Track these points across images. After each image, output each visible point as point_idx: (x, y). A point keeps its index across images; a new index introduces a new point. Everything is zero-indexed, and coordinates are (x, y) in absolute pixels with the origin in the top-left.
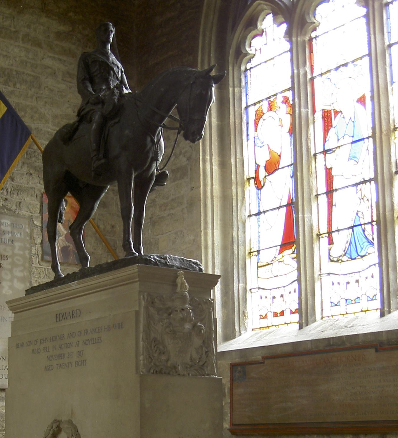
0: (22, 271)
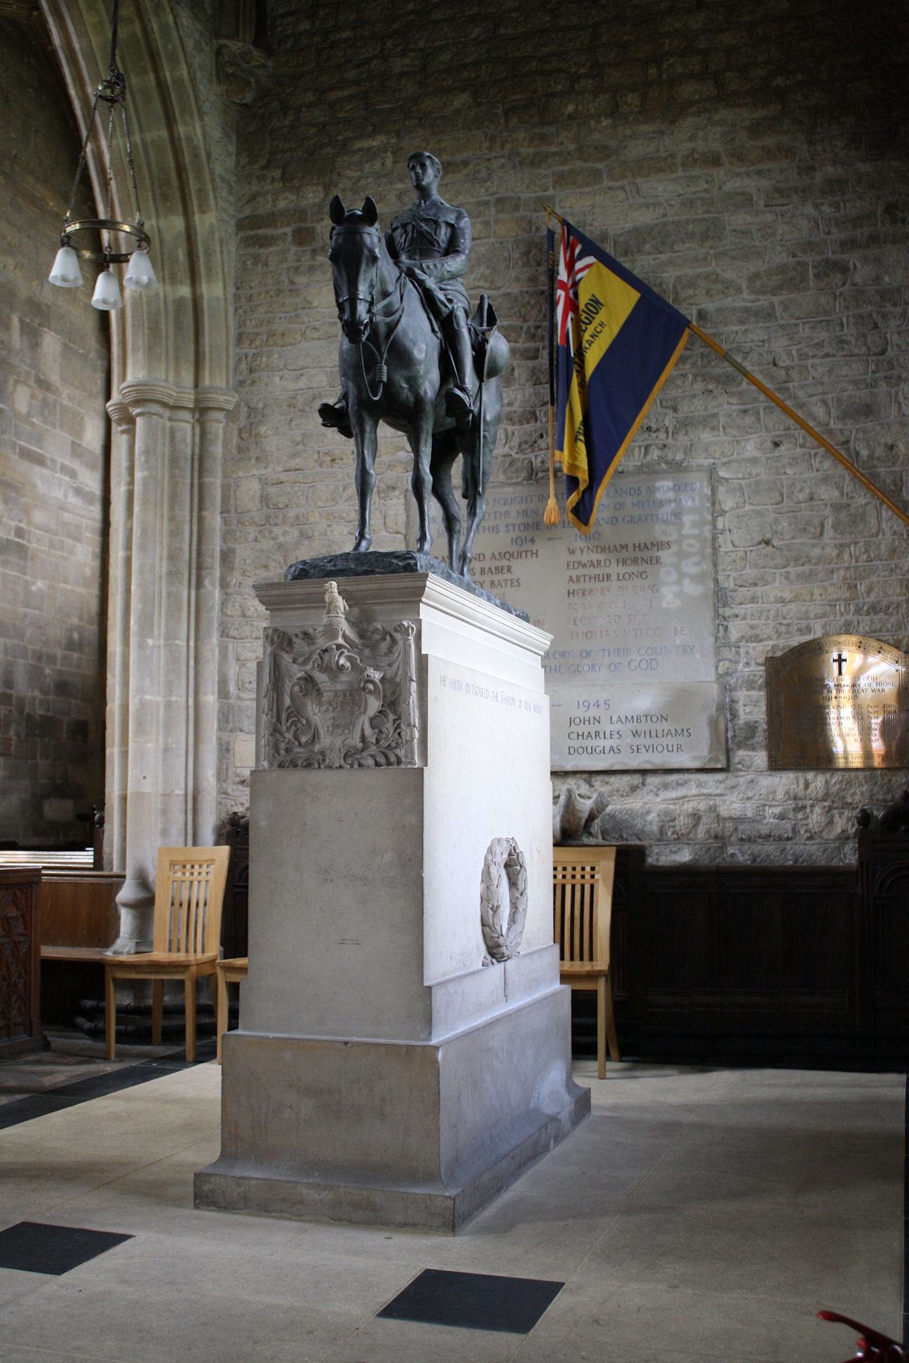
0: (697, 564)
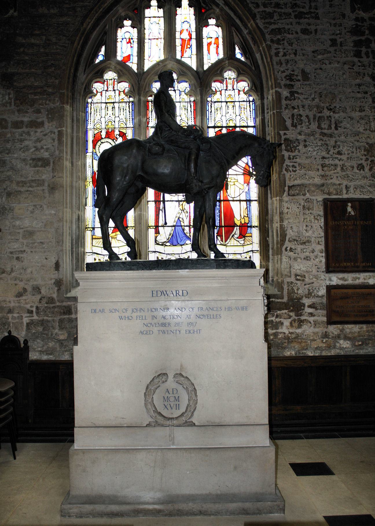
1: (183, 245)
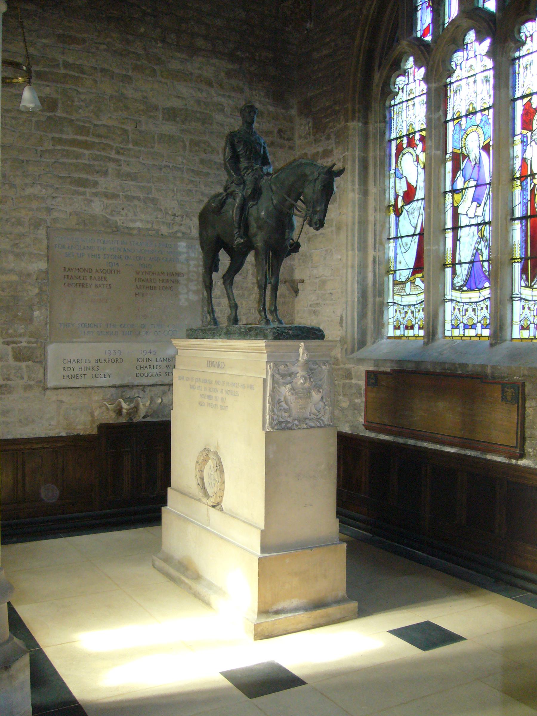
0: (196, 285)
1: (481, 289)
